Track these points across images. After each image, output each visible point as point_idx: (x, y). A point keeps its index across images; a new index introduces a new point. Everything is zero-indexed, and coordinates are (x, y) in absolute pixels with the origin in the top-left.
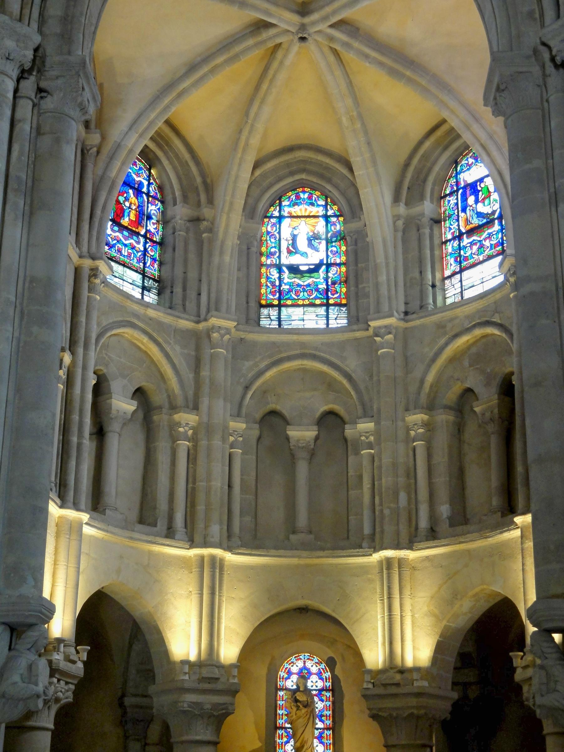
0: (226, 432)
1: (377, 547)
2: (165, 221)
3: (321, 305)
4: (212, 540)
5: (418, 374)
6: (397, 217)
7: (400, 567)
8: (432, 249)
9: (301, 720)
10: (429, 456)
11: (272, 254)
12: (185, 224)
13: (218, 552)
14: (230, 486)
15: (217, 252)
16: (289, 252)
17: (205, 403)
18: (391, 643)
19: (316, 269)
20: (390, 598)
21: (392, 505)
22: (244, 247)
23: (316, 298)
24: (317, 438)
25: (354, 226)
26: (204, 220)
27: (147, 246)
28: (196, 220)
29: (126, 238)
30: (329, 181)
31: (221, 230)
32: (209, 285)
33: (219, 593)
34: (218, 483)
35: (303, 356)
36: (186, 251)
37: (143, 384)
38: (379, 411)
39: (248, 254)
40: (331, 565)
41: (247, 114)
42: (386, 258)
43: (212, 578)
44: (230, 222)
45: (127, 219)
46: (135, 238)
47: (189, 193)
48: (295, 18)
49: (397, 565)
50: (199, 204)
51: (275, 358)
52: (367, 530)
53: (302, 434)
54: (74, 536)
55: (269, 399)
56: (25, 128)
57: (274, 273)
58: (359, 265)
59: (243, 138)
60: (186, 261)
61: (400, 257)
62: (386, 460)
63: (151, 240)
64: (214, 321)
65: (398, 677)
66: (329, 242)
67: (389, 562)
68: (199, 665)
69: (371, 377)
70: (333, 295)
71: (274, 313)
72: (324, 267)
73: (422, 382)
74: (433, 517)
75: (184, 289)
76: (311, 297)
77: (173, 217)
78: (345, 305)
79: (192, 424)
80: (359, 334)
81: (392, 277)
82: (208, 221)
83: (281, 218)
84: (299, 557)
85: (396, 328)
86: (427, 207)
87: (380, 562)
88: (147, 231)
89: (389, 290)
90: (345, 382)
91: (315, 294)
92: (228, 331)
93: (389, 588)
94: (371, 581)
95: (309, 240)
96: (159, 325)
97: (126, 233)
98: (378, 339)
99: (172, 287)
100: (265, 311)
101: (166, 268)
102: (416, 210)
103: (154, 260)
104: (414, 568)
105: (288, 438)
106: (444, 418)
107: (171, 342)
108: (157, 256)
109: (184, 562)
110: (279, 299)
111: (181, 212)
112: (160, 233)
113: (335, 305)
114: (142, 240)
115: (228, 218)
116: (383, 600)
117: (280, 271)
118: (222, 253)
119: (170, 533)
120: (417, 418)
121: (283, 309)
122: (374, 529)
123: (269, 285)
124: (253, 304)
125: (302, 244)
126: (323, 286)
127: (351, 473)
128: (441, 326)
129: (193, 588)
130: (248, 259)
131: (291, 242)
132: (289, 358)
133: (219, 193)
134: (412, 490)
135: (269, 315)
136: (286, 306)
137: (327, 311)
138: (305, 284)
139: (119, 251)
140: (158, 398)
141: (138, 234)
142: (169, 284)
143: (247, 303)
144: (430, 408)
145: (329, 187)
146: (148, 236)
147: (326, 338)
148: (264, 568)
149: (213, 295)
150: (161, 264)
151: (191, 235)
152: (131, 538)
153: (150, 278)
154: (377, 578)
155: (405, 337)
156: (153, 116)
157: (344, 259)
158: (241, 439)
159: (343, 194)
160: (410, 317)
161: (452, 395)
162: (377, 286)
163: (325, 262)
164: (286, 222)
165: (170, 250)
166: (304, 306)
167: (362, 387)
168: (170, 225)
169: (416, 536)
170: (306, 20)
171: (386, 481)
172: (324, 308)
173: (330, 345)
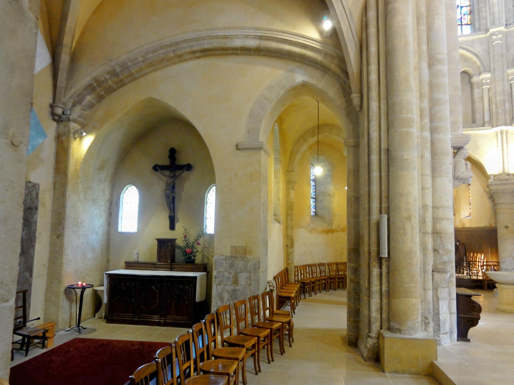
1: (494, 125)
7: (506, 133)
38: (494, 69)
65: (507, 177)
72: (459, 8)
78: (470, 24)
89: (499, 15)
90: (474, 58)
93: (502, 142)
113: (465, 24)
160: (508, 26)
173: (467, 42)
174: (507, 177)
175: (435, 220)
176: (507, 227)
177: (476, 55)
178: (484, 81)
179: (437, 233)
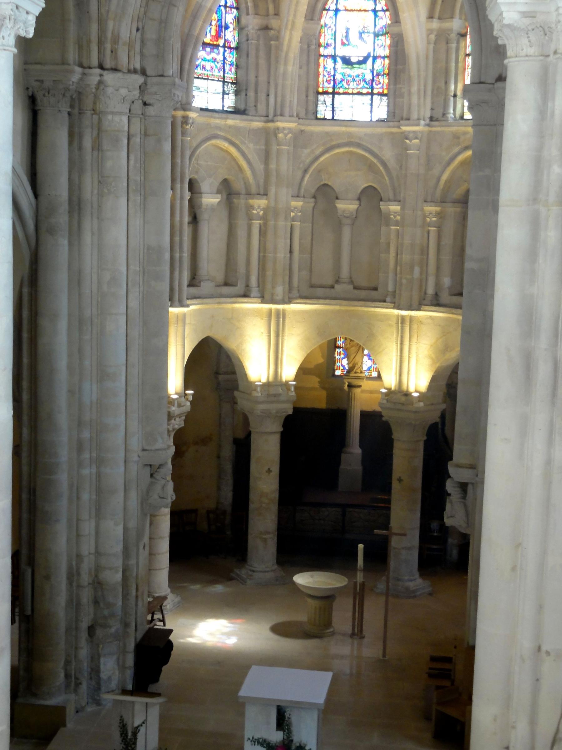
0: (289, 209)
2: (241, 28)
3: (367, 94)
4: (278, 298)
5: (436, 171)
6: (430, 32)
7: (410, 322)
8: (457, 62)
9: (353, 348)
12: (256, 33)
13: (280, 307)
14: (291, 252)
15: (282, 62)
16: (343, 44)
17: (272, 190)
18: (400, 375)
19: (363, 61)
20: (402, 344)
21: (408, 277)
22: (306, 46)
23: (362, 88)
24: (357, 210)
26: (272, 29)
27: (226, 54)
28: (266, 28)
29: (208, 54)
31: (286, 43)
33: (283, 334)
34: (282, 255)
36: (257, 57)
37: (226, 177)
39: (309, 51)
40: (364, 311)
42: (419, 71)
44: (292, 40)
45: (209, 36)
46: (216, 51)
49: (408, 321)
50: (267, 15)
51: (328, 146)
52: (390, 288)
53: (347, 207)
54: (180, 324)
55: (323, 177)
56: (137, 140)
57: (330, 62)
58: (398, 67)
61: (431, 67)
62: (407, 241)
63: (229, 48)
64: (280, 124)
65: (403, 399)
66: (376, 35)
67: (403, 319)
68: (267, 385)
69: (401, 167)
70: (377, 85)
71: (329, 98)
72: (370, 60)
75: (256, 92)
76: (360, 87)
77: (247, 26)
79: (263, 206)
80: (394, 130)
81: (422, 87)
82: (274, 30)
83: (337, 11)
84: (341, 305)
85: (422, 132)
87: (398, 316)
88: (226, 41)
91: (362, 83)
94: (390, 326)
95: (361, 34)
96: (237, 130)
97: (208, 49)
98: (407, 141)
99: (246, 90)
100: (321, 98)
101: (241, 72)
102: (446, 25)
103: (232, 65)
104: (421, 322)
106: (452, 210)
107: (246, 142)
108: (234, 61)
109: (257, 313)
110: (334, 88)
111: (253, 22)
112: (236, 38)
113: (379, 94)
114: (221, 50)
115: (291, 33)
116: (397, 343)
117: (335, 62)
118: (286, 64)
119: (246, 295)
121: (336, 96)
122: (396, 288)
123: (326, 74)
124: (311, 97)
125: (354, 36)
126: (369, 77)
127: (383, 240)
128: (456, 137)
130: (308, 56)
131: (344, 35)
132: (339, 146)
134: (424, 264)
135: (325, 102)
136: (338, 93)
137: (372, 99)
138: (355, 74)
139: (204, 68)
141: (218, 46)
142: (244, 88)
143: (307, 97)
144: (443, 201)
146: (227, 45)
147: (368, 130)
148: (315, 311)
149: (279, 100)
150: (237, 67)
151: (261, 42)
152: (219, 303)
153: (228, 82)
154: (395, 325)
155: (430, 139)
157: (387, 52)
158: (300, 214)
160: (434, 123)
161: (459, 192)
163: (372, 55)
164: (339, 14)
165: (244, 56)
166: (353, 94)
167: (394, 174)
168: (245, 32)
169: (424, 299)
171: (406, 257)
172: (370, 97)
174: (403, 399)
175: (98, 569)
176: (400, 480)
178: (392, 216)
179: (99, 583)
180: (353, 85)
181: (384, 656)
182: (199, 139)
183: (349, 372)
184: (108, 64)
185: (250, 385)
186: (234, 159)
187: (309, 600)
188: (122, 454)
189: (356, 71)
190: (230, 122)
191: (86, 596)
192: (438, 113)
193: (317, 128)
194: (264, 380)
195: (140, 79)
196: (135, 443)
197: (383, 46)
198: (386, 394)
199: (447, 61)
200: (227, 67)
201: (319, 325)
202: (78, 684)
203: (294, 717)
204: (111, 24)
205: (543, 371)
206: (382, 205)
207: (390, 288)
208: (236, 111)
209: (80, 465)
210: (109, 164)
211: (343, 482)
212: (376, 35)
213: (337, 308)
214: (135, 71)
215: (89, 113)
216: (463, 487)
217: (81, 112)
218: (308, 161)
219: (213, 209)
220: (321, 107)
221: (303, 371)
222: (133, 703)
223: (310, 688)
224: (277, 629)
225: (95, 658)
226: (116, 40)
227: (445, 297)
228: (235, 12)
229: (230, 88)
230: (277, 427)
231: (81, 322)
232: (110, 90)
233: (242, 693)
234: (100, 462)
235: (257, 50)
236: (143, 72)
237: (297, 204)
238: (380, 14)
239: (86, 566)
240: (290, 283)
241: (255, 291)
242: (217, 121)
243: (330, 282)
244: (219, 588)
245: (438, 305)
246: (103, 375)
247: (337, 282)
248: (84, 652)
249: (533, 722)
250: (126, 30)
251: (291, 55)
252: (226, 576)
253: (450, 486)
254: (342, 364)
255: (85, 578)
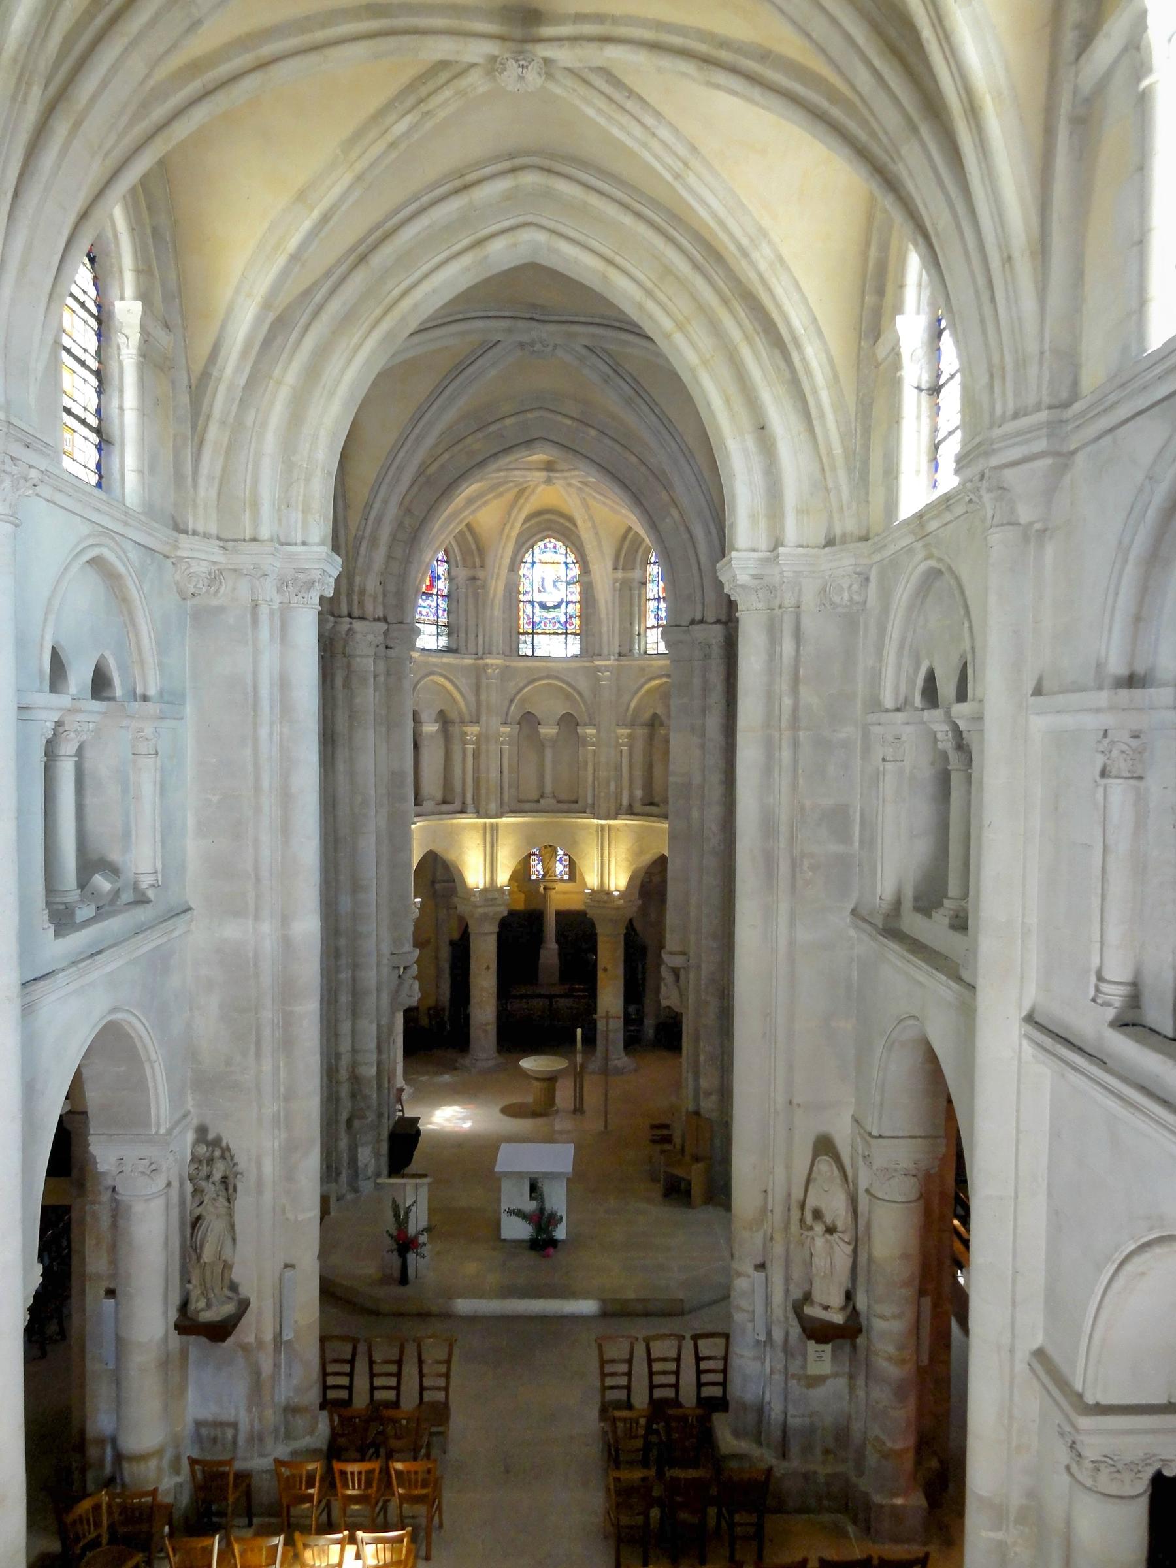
2: (451, 578)
6: (615, 581)
10: (631, 755)
11: (527, 592)
16: (540, 591)
17: (483, 719)
25: (585, 579)
28: (474, 579)
30: (569, 539)
31: (492, 591)
32: (484, 631)
34: (494, 774)
35: (548, 677)
36: (467, 604)
41: (509, 514)
43: (491, 838)
44: (497, 588)
47: (466, 554)
48: (544, 474)
52: (590, 801)
53: (548, 731)
56: (381, 679)
57: (529, 608)
59: (506, 531)
60: (467, 611)
62: (603, 760)
64: (489, 661)
66: (568, 584)
67: (602, 826)
68: (485, 890)
71: (529, 638)
73: (628, 705)
74: (631, 796)
80: (587, 664)
83: (533, 563)
86: (637, 574)
90: (577, 697)
91: (558, 625)
92: (498, 666)
95: (554, 582)
100: (522, 638)
102: (630, 575)
105: (538, 733)
106: (641, 732)
109: (474, 826)
111: (462, 573)
113: (572, 634)
119: (462, 812)
120: (625, 731)
125: (548, 584)
126: (563, 619)
127: (581, 759)
128: (642, 669)
129: (479, 841)
133: (489, 561)
140: (453, 715)
141: (432, 594)
145: (568, 544)
147: (564, 665)
148: (524, 824)
149: (487, 639)
156: (442, 537)
157: (578, 598)
159: (578, 550)
161: (647, 716)
162: (601, 633)
170: (551, 474)
171: (603, 774)
175: (354, 1065)
177: (580, 694)
180: (550, 626)
181: (606, 1127)
182: (418, 677)
183: (544, 876)
184: (356, 613)
185: (469, 892)
186: (449, 692)
187: (536, 1083)
188: (374, 959)
189: (551, 615)
190: (445, 660)
191: (344, 1091)
192: (625, 650)
193: (521, 664)
194: (481, 886)
195: (384, 626)
196: (386, 949)
197: (574, 592)
198: (590, 894)
199: (631, 605)
200: (440, 612)
201: (529, 836)
202: (338, 1174)
203: (546, 1188)
204: (358, 579)
205: (784, 868)
206: (580, 729)
207: (590, 801)
208: (449, 650)
209: (337, 971)
210: (358, 700)
211: (543, 977)
212: (568, 584)
213: (544, 819)
214: (378, 619)
215: (339, 656)
216: (676, 972)
217: (332, 656)
218: (514, 691)
219: (431, 736)
220: (522, 646)
221: (513, 878)
222: (405, 1184)
223: (555, 1159)
224: (506, 1111)
225: (353, 1149)
226: (362, 592)
227: (638, 807)
228: (446, 565)
229: (443, 630)
230: (494, 928)
231: (336, 841)
232: (358, 637)
233: (497, 1169)
234: (355, 967)
235: (467, 597)
236: (385, 620)
237: (505, 730)
238: (570, 566)
239: (345, 1062)
240: (502, 799)
241: (471, 808)
242: (434, 659)
243: (536, 797)
244: (447, 1078)
245: (633, 814)
246: (356, 887)
247: (542, 797)
248: (343, 1143)
249: (788, 1167)
250: (372, 585)
251: (497, 602)
252: (452, 1067)
253: (664, 972)
254: (537, 869)
255: (344, 1074)
